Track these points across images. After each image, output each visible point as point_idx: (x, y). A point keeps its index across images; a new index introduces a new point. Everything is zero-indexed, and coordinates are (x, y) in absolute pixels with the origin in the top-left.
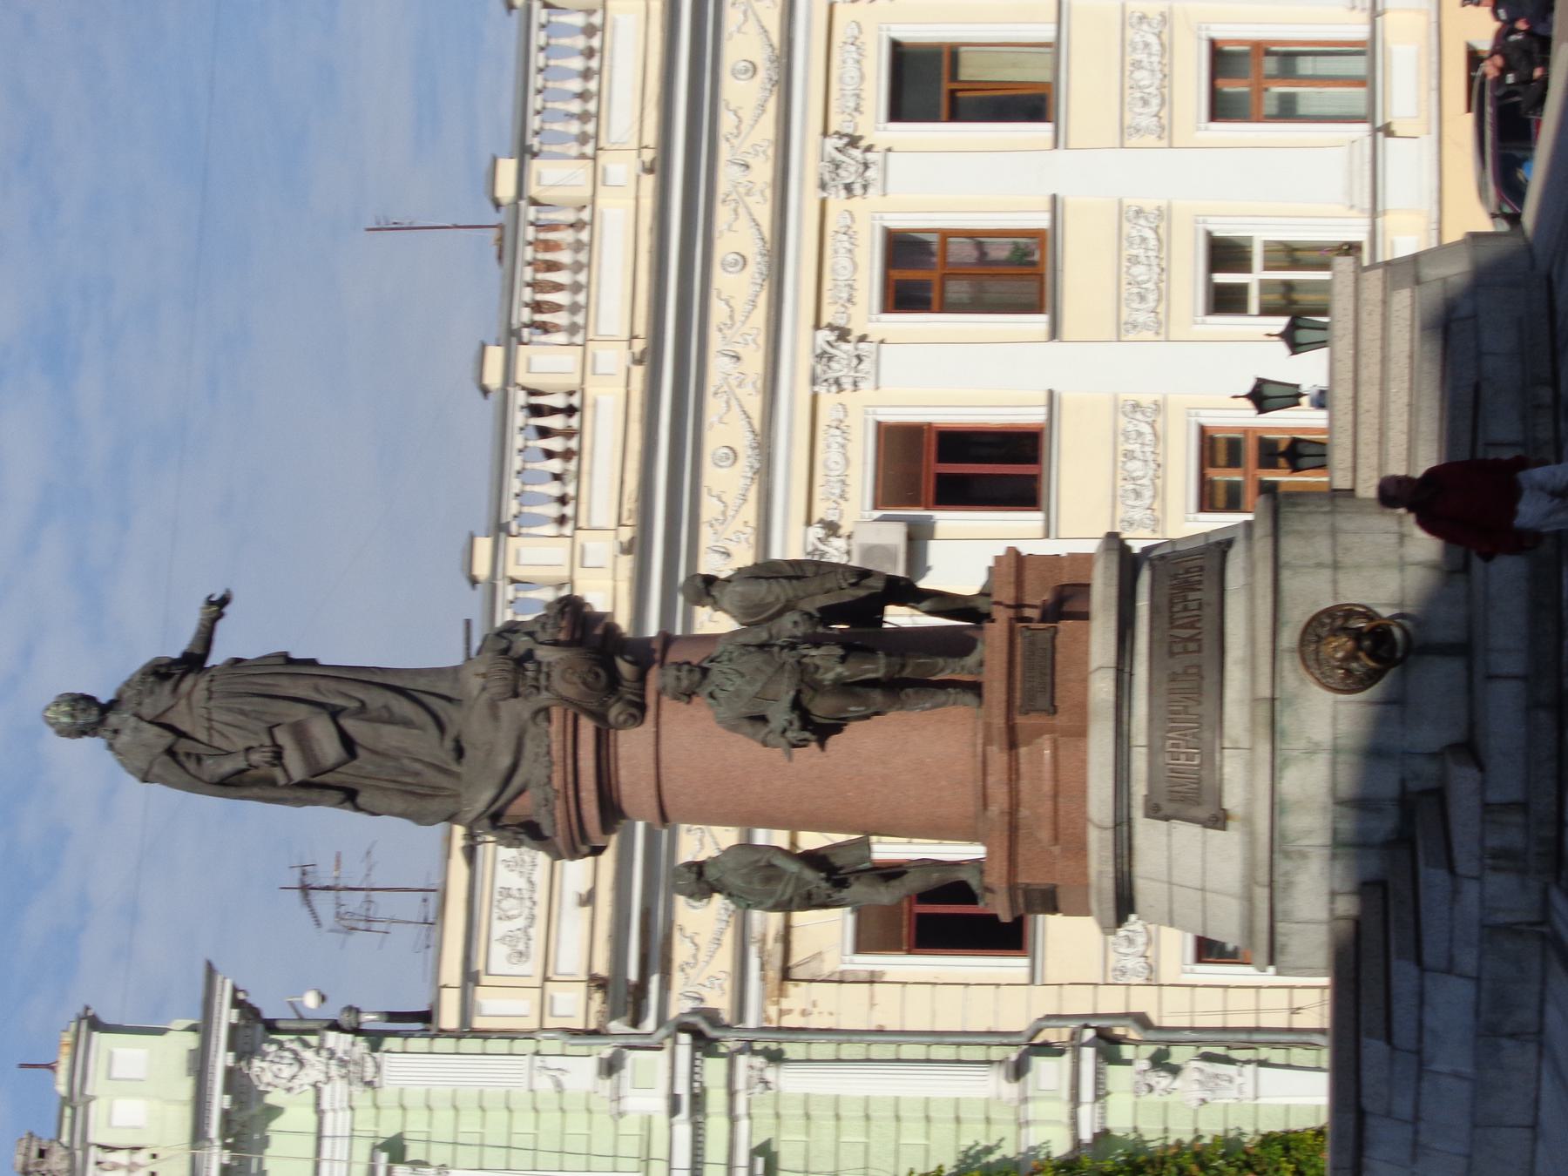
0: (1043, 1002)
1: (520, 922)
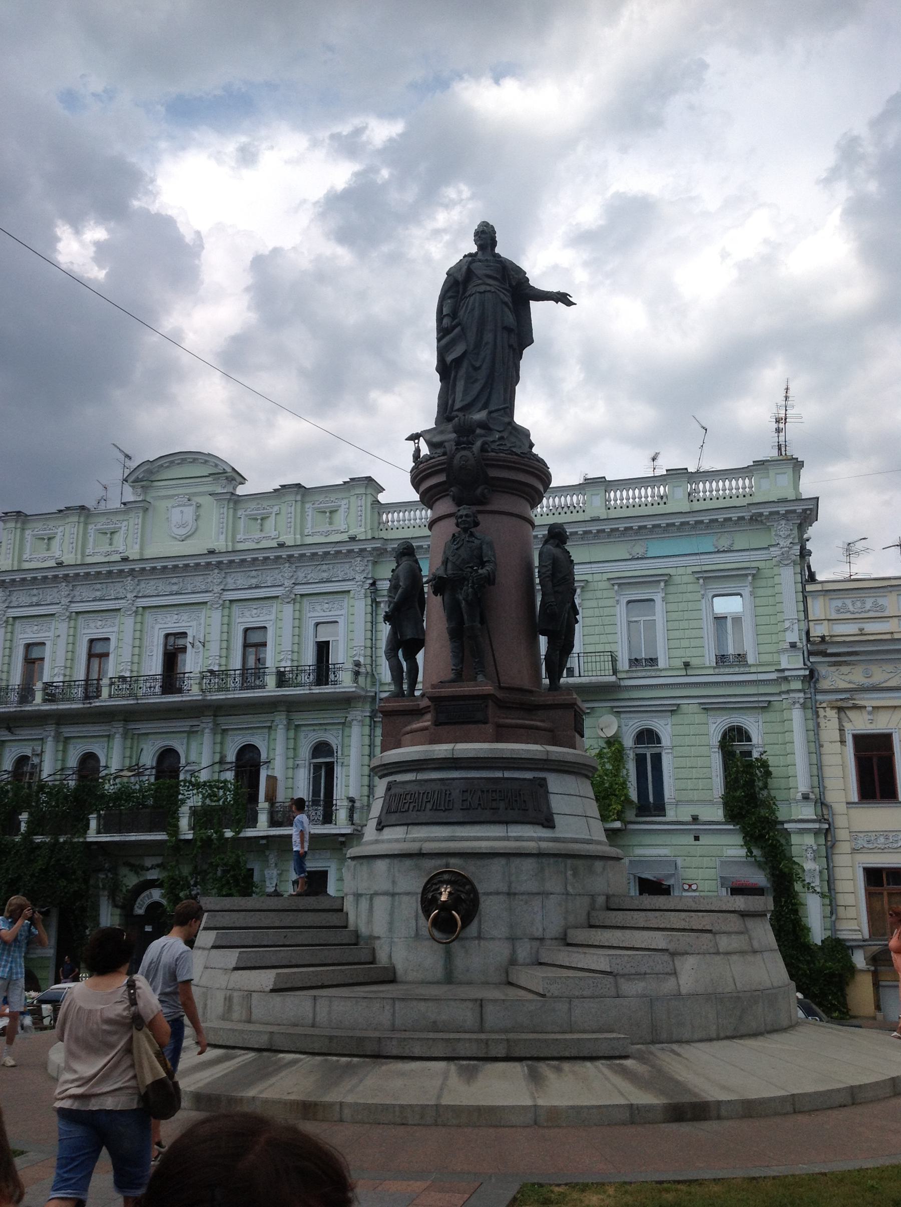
0: (839, 808)
1: (852, 609)
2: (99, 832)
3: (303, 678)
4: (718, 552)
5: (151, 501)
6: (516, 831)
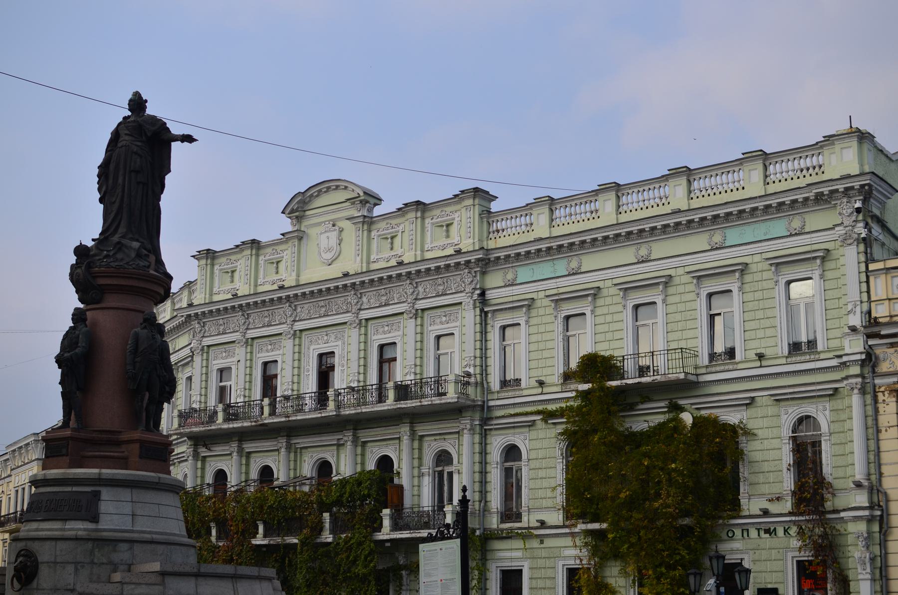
2: (265, 536)
3: (427, 390)
4: (791, 235)
5: (305, 230)
6: (70, 525)
